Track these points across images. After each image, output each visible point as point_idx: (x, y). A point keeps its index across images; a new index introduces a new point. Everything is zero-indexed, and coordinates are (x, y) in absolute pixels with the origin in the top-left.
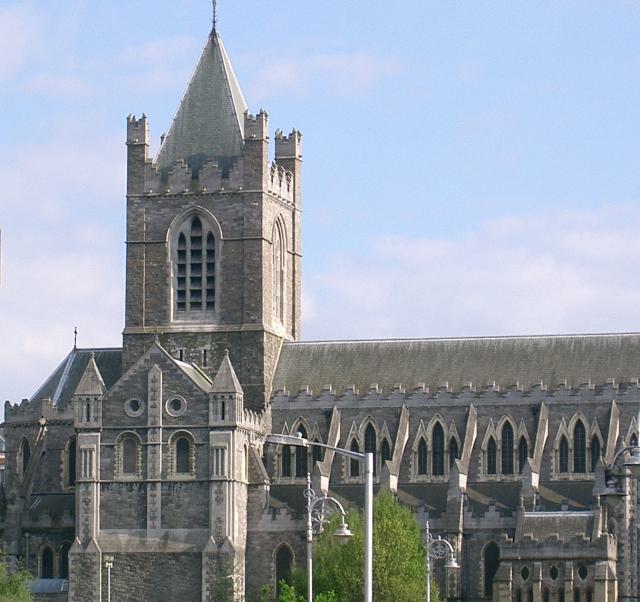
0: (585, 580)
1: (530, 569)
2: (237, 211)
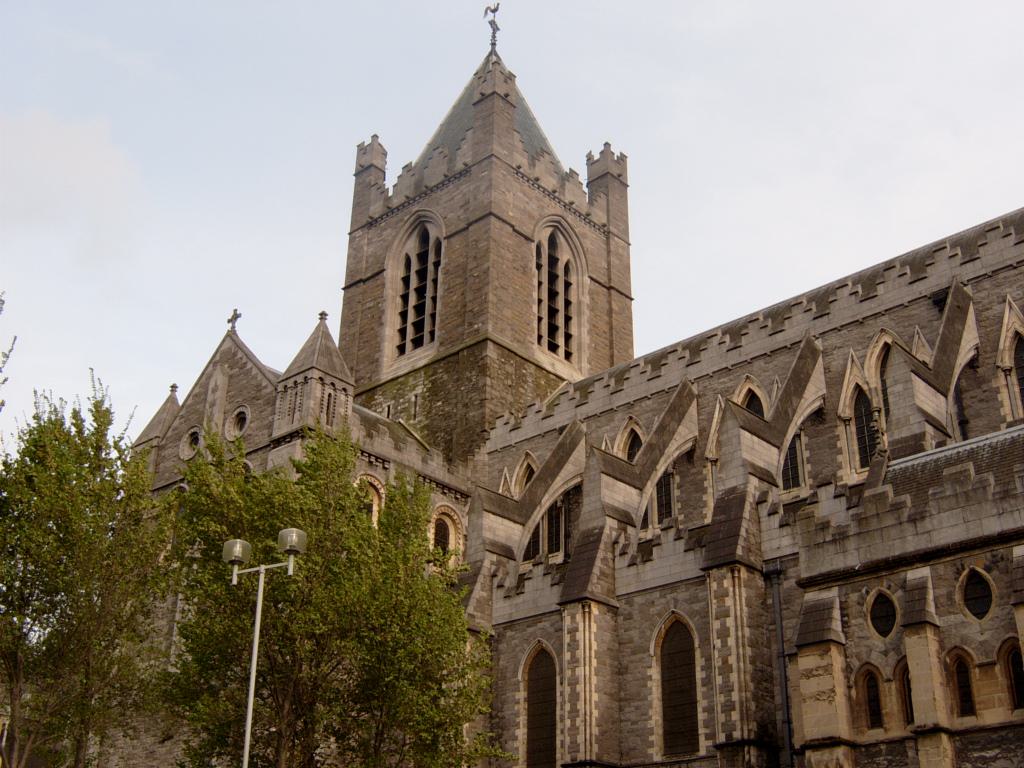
1: (896, 597)
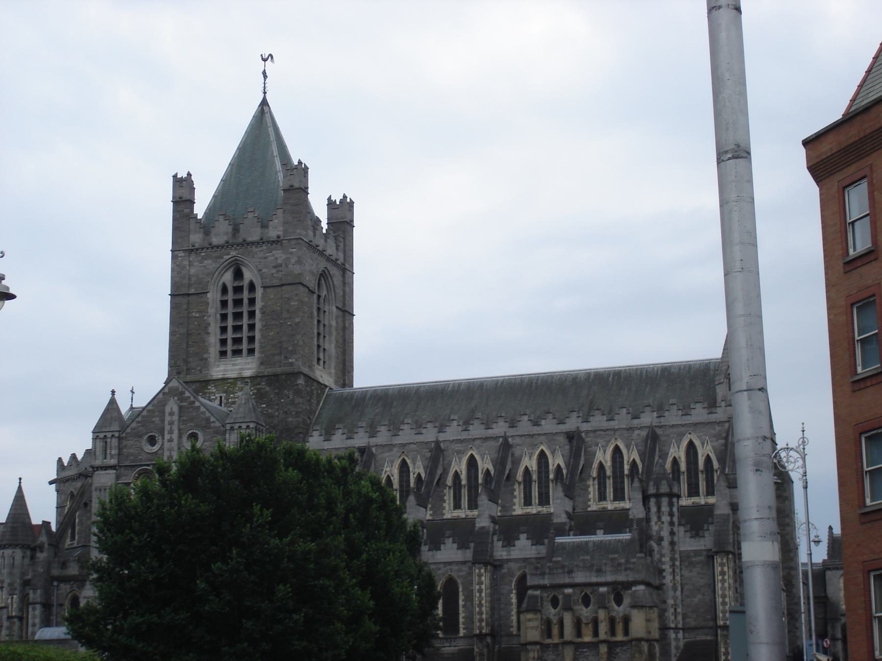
0: (622, 607)
1: (560, 597)
2: (276, 259)
